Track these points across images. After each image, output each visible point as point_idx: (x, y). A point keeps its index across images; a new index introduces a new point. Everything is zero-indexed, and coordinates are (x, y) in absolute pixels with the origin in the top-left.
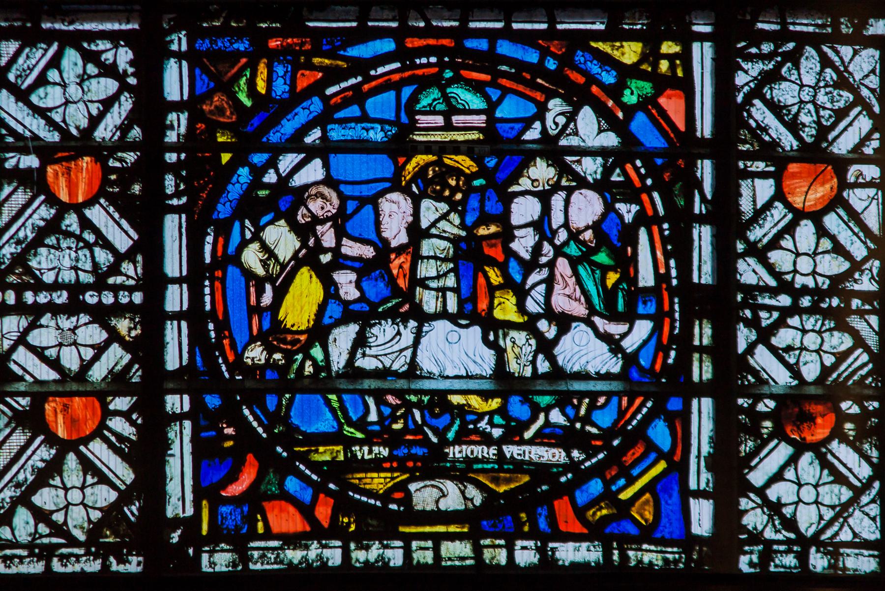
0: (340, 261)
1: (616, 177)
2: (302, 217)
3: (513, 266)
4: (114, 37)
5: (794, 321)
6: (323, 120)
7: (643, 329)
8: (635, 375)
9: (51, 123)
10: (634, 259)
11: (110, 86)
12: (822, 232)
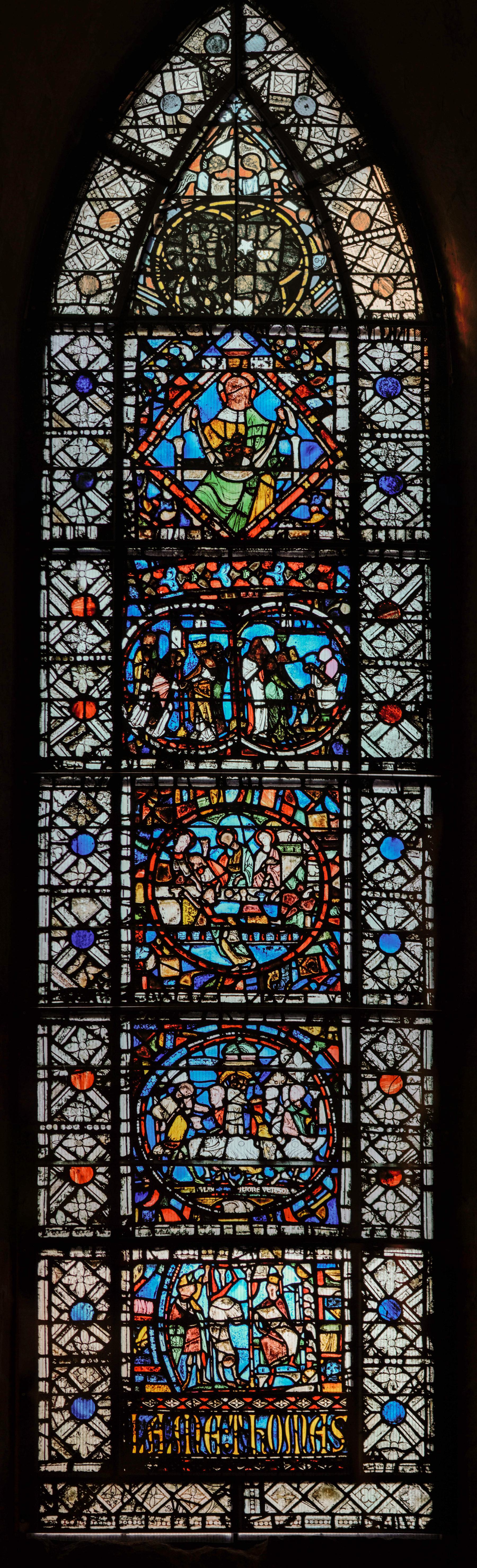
0: (194, 1113)
1: (310, 1080)
2: (178, 1095)
3: (267, 1115)
4: (100, 1024)
5: (385, 1138)
6: (187, 1057)
7: (321, 1141)
8: (318, 1159)
9: (73, 1058)
10: (318, 1113)
11: (98, 1043)
12: (396, 1102)
